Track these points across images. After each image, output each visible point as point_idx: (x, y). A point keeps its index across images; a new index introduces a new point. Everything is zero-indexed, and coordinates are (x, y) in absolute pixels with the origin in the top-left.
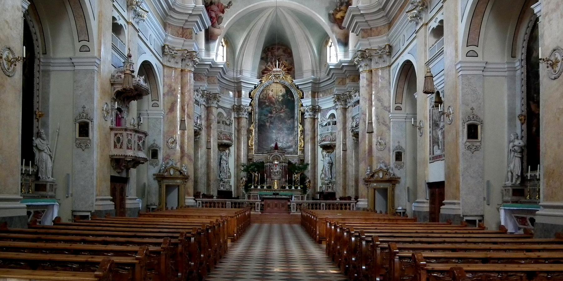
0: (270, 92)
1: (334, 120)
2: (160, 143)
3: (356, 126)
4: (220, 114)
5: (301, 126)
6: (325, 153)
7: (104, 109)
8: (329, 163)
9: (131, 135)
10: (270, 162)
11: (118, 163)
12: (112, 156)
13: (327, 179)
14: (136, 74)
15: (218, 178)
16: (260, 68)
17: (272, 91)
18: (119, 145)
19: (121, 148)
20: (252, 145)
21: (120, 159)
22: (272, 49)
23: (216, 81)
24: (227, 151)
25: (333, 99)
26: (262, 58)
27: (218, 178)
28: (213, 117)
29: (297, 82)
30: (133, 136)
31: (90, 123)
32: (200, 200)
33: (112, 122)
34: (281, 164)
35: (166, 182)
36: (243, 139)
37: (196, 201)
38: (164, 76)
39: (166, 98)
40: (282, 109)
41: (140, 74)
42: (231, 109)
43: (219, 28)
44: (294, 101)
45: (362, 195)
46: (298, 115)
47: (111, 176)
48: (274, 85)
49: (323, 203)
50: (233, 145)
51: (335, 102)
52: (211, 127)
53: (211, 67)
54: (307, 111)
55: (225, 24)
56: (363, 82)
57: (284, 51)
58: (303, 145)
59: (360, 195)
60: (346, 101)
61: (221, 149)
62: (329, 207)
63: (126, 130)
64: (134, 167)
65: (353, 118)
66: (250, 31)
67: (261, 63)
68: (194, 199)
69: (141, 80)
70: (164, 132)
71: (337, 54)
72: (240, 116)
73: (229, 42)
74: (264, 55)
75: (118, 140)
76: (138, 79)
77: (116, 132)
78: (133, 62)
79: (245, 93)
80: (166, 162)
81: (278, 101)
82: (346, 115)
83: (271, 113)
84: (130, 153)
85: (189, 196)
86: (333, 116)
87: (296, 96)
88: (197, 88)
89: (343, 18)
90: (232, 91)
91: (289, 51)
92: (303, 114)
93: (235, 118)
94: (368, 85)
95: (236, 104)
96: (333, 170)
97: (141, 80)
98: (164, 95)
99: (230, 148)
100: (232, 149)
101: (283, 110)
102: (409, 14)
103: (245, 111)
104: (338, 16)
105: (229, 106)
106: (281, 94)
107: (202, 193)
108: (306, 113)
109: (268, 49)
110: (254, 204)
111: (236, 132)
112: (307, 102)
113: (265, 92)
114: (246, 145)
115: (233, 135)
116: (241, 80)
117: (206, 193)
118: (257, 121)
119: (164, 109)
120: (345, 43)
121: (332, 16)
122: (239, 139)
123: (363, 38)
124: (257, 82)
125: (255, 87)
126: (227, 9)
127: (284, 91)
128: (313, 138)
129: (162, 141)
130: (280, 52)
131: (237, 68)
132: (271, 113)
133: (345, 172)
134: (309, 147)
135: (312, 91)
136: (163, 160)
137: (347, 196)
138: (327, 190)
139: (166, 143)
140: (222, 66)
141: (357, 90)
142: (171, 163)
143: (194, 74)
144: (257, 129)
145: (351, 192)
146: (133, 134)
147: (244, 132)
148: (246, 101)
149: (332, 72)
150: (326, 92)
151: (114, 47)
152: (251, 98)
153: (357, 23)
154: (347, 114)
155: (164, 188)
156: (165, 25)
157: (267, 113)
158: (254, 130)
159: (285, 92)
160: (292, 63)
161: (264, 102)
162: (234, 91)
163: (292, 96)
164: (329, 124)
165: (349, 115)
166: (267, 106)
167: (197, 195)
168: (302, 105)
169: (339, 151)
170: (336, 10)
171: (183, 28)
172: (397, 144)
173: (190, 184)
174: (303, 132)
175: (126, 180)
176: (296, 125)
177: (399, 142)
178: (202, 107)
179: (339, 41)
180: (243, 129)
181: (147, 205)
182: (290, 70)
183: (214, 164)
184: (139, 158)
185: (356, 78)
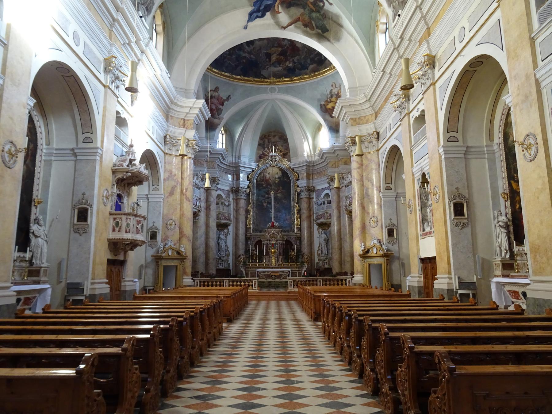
0: (267, 175)
1: (329, 199)
2: (159, 225)
3: (349, 205)
4: (219, 196)
6: (320, 230)
7: (105, 195)
8: (325, 240)
9: (130, 219)
10: (267, 240)
11: (116, 246)
12: (110, 239)
13: (323, 255)
14: (137, 162)
15: (217, 257)
16: (257, 153)
18: (117, 229)
19: (119, 231)
21: (118, 242)
22: (269, 136)
23: (216, 166)
24: (226, 231)
25: (328, 180)
26: (259, 145)
27: (217, 257)
28: (212, 199)
30: (132, 219)
31: (89, 209)
32: (198, 279)
33: (112, 207)
34: (279, 242)
35: (164, 263)
36: (242, 218)
37: (194, 281)
38: (165, 163)
39: (167, 183)
40: (278, 190)
41: (141, 162)
43: (219, 119)
45: (357, 271)
46: (294, 196)
47: (108, 259)
48: (270, 168)
49: (320, 279)
50: (232, 225)
52: (210, 209)
56: (354, 165)
57: (280, 138)
59: (355, 271)
61: (220, 228)
62: (325, 283)
63: (125, 214)
64: (132, 249)
67: (258, 149)
68: (192, 279)
69: (142, 169)
70: (163, 214)
72: (239, 197)
75: (117, 224)
76: (139, 166)
77: (115, 217)
78: (135, 151)
80: (164, 243)
81: (275, 183)
83: (268, 194)
84: (129, 236)
85: (187, 275)
86: (327, 195)
87: (292, 178)
88: (197, 172)
89: (333, 108)
91: (285, 137)
92: (299, 194)
93: (233, 199)
94: (359, 168)
95: (235, 186)
96: (328, 247)
97: (142, 169)
98: (164, 180)
100: (231, 228)
102: (393, 105)
104: (329, 106)
105: (227, 188)
106: (277, 176)
107: (200, 272)
108: (302, 194)
109: (265, 136)
110: (252, 282)
112: (302, 183)
113: (262, 175)
114: (244, 224)
115: (232, 216)
117: (204, 272)
118: (255, 202)
119: (164, 192)
121: (324, 107)
122: (237, 219)
123: (352, 126)
124: (254, 165)
125: (253, 171)
127: (280, 174)
128: (309, 217)
129: (161, 223)
130: (277, 138)
134: (305, 225)
136: (162, 242)
137: (343, 271)
138: (324, 265)
139: (165, 225)
140: (222, 152)
141: (350, 173)
142: (169, 244)
143: (195, 160)
144: (255, 209)
145: (347, 268)
146: (132, 217)
147: (242, 212)
148: (244, 182)
149: (325, 156)
151: (117, 138)
152: (249, 180)
153: (346, 113)
154: (341, 194)
155: (161, 269)
160: (287, 148)
161: (261, 184)
162: (233, 175)
164: (324, 203)
166: (264, 188)
167: (194, 275)
168: (298, 186)
170: (327, 101)
171: (184, 120)
172: (389, 222)
173: (188, 263)
174: (299, 211)
175: (122, 263)
176: (292, 204)
177: (391, 219)
180: (242, 209)
181: (144, 287)
182: (286, 154)
183: (213, 243)
184: (137, 240)
185: (348, 161)
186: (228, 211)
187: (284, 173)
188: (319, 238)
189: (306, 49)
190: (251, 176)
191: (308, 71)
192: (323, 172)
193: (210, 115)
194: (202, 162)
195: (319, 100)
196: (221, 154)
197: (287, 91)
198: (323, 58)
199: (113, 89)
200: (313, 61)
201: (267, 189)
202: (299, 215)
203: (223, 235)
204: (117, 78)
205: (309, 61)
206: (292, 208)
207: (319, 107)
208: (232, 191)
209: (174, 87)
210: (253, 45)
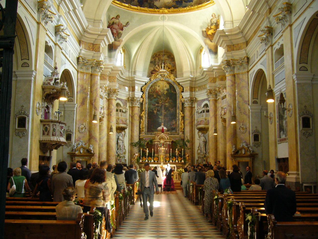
0: (157, 87)
1: (208, 109)
4: (118, 105)
5: (182, 113)
6: (200, 134)
8: (204, 142)
13: (202, 154)
16: (149, 69)
20: (143, 128)
23: (116, 80)
24: (123, 133)
26: (151, 62)
28: (113, 107)
29: (178, 80)
36: (136, 123)
42: (126, 101)
43: (119, 41)
46: (179, 104)
48: (160, 82)
50: (128, 128)
51: (208, 95)
52: (111, 115)
54: (186, 101)
55: (125, 38)
57: (168, 57)
58: (183, 128)
61: (118, 131)
65: (222, 108)
66: (142, 43)
67: (150, 66)
71: (209, 60)
72: (134, 105)
73: (127, 51)
74: (153, 60)
81: (163, 94)
83: (158, 103)
86: (206, 105)
87: (178, 90)
90: (127, 87)
92: (183, 104)
93: (129, 107)
95: (131, 96)
96: (207, 147)
99: (126, 130)
100: (127, 131)
101: (167, 101)
105: (124, 98)
106: (165, 89)
108: (186, 103)
109: (156, 55)
111: (130, 118)
112: (186, 95)
113: (153, 87)
114: (138, 128)
116: (135, 79)
118: (147, 109)
120: (215, 52)
121: (205, 33)
122: (132, 123)
124: (147, 80)
125: (146, 84)
126: (125, 27)
127: (168, 86)
128: (192, 122)
130: (165, 57)
131: (132, 70)
132: (158, 103)
133: (216, 148)
134: (187, 129)
135: (190, 87)
138: (203, 162)
140: (121, 69)
144: (147, 115)
147: (137, 118)
148: (138, 94)
149: (205, 74)
150: (201, 88)
152: (143, 92)
154: (217, 105)
156: (80, 42)
157: (154, 103)
158: (144, 116)
159: (169, 87)
160: (174, 65)
162: (129, 87)
163: (175, 91)
164: (204, 111)
165: (219, 105)
166: (155, 98)
168: (183, 97)
169: (211, 133)
170: (208, 28)
174: (183, 118)
178: (105, 100)
179: (210, 51)
180: (136, 115)
182: (173, 71)
186: (125, 116)
188: (198, 140)
190: (144, 89)
192: (204, 86)
193: (113, 40)
194: (105, 77)
195: (201, 27)
196: (121, 71)
197: (174, 20)
199: (44, 25)
201: (157, 99)
202: (183, 121)
203: (121, 136)
204: (47, 16)
206: (177, 115)
207: (202, 33)
208: (129, 100)
209: (86, 18)
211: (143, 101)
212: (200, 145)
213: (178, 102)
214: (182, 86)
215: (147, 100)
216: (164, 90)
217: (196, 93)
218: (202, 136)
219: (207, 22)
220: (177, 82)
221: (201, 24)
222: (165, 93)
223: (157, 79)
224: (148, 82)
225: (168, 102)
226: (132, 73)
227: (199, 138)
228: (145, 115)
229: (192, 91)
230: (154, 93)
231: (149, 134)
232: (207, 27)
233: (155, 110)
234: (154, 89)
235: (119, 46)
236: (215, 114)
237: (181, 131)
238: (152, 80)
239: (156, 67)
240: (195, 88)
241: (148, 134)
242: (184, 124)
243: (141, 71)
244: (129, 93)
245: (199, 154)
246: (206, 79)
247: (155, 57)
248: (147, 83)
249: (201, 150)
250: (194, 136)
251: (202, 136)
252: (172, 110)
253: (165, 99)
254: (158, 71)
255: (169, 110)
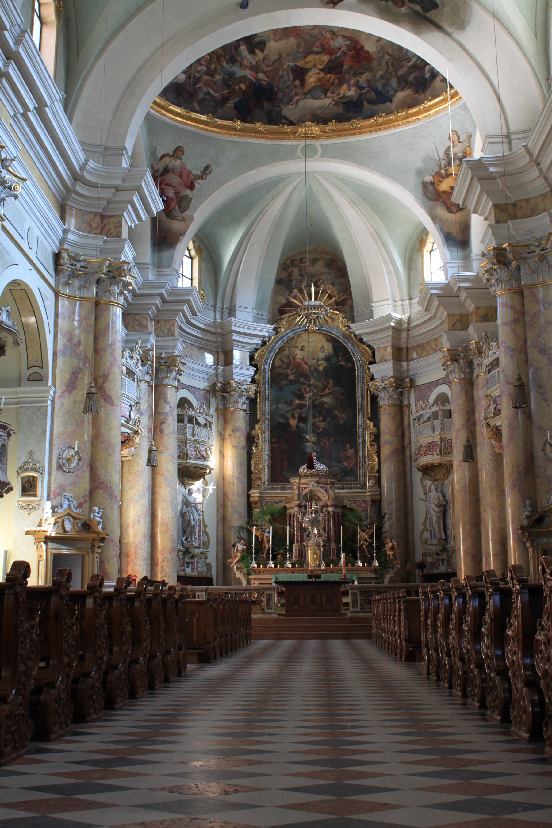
0: (298, 352)
1: (447, 407)
5: (371, 424)
6: (428, 483)
13: (435, 542)
16: (274, 302)
17: (302, 349)
25: (443, 361)
26: (279, 282)
29: (358, 328)
40: (325, 387)
44: (352, 370)
46: (362, 401)
48: (305, 336)
53: (164, 301)
60: (470, 364)
67: (276, 293)
79: (241, 356)
81: (316, 370)
82: (472, 394)
83: (301, 397)
86: (443, 399)
90: (210, 352)
92: (374, 399)
93: (217, 410)
101: (327, 391)
103: (240, 396)
105: (203, 385)
106: (322, 355)
109: (292, 262)
112: (383, 370)
113: (286, 352)
116: (233, 328)
118: (268, 416)
121: (431, 188)
124: (266, 330)
125: (264, 343)
126: (200, 181)
127: (328, 348)
130: (320, 267)
135: (393, 347)
150: (424, 348)
152: (255, 366)
154: (475, 393)
159: (331, 351)
160: (346, 288)
163: (349, 359)
165: (479, 394)
168: (372, 379)
170: (438, 174)
187: (339, 348)
189: (387, 57)
190: (261, 357)
191: (393, 106)
195: (420, 173)
197: (343, 155)
198: (428, 75)
200: (403, 83)
201: (297, 386)
205: (394, 83)
206: (360, 431)
207: (420, 188)
210: (262, 51)
211: (256, 393)
212: (429, 516)
213: (359, 393)
214: (369, 346)
215: (267, 390)
216: (318, 360)
217: (413, 365)
218: (433, 488)
219: (436, 157)
220: (355, 335)
221: (419, 164)
222: (321, 368)
223: (297, 327)
224: (270, 338)
225: (329, 393)
226: (222, 312)
227: (424, 497)
228: (264, 432)
229: (401, 361)
230: (288, 368)
231: (276, 489)
232: (437, 170)
233: (293, 417)
234: (288, 357)
235: (184, 233)
236: (468, 420)
237: (370, 478)
238: (283, 330)
239: (293, 294)
240: (407, 349)
241: (272, 489)
242: (379, 457)
243: (251, 306)
244: (216, 369)
245: (427, 542)
246: (439, 322)
247: (289, 267)
248: (269, 341)
249: (431, 532)
250: (409, 491)
251: (433, 488)
252: (342, 416)
253: (320, 384)
254: (298, 306)
255: (335, 417)
